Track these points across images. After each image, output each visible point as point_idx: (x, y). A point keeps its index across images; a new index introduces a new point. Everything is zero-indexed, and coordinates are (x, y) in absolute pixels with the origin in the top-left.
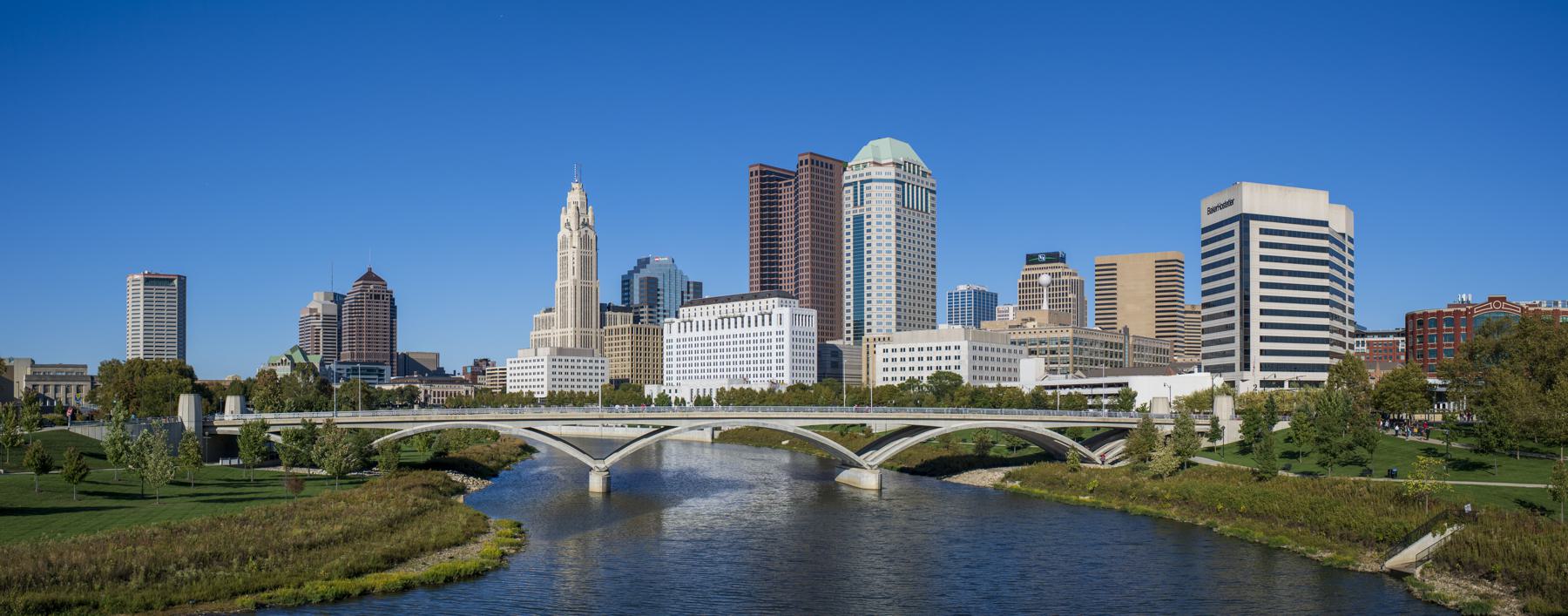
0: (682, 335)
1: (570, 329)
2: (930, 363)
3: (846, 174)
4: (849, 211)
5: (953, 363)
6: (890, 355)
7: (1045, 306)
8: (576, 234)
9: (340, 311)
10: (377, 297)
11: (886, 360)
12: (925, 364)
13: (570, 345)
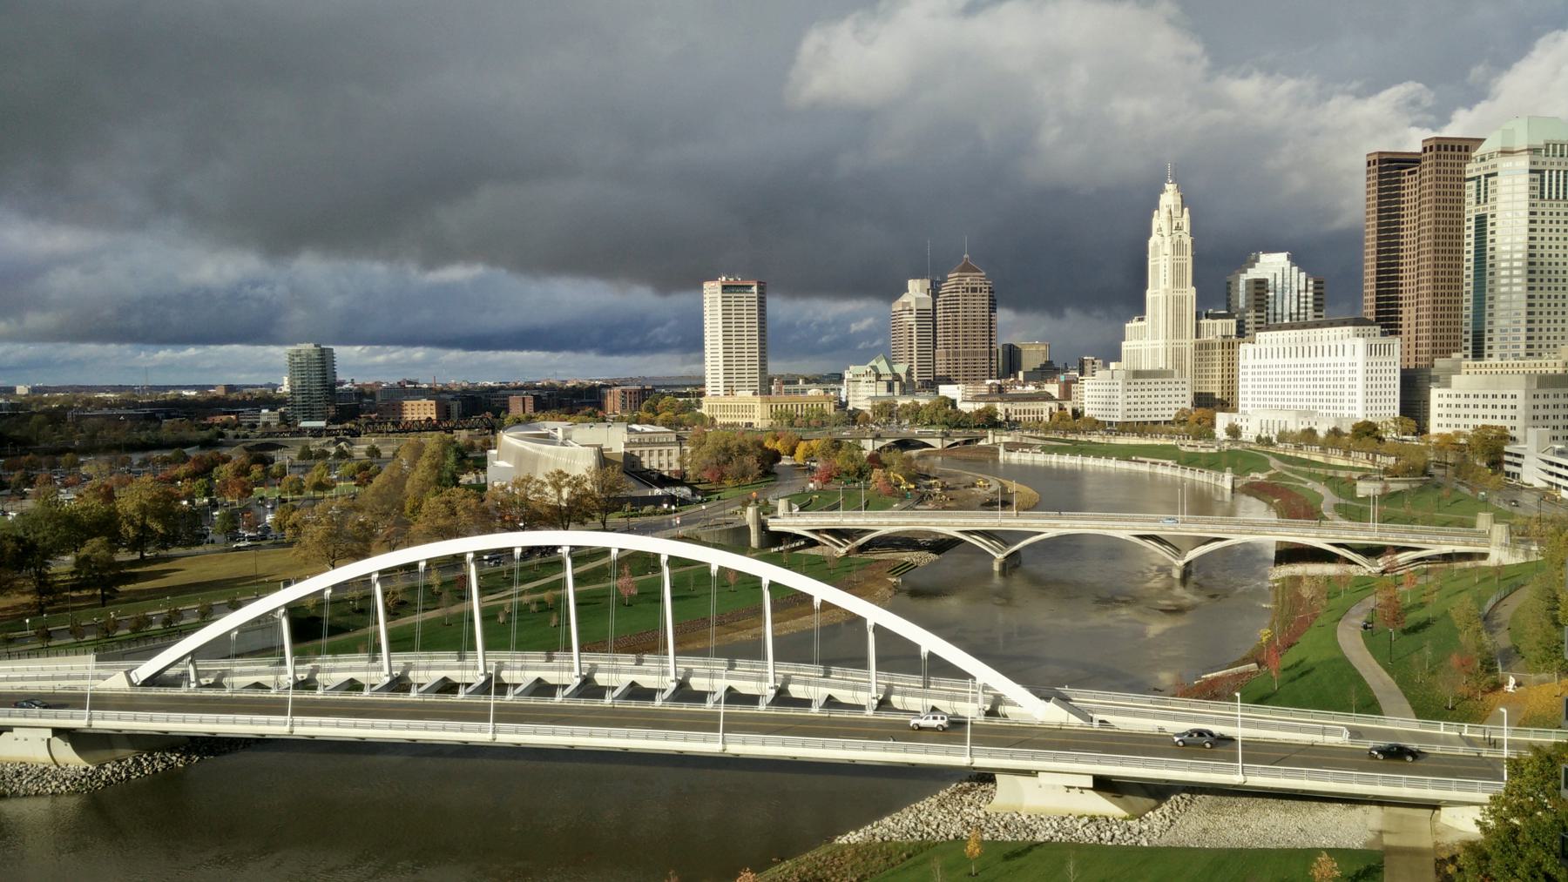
0: (1257, 362)
1: (1161, 342)
3: (1468, 167)
4: (1471, 210)
8: (1168, 240)
9: (934, 305)
10: (974, 290)
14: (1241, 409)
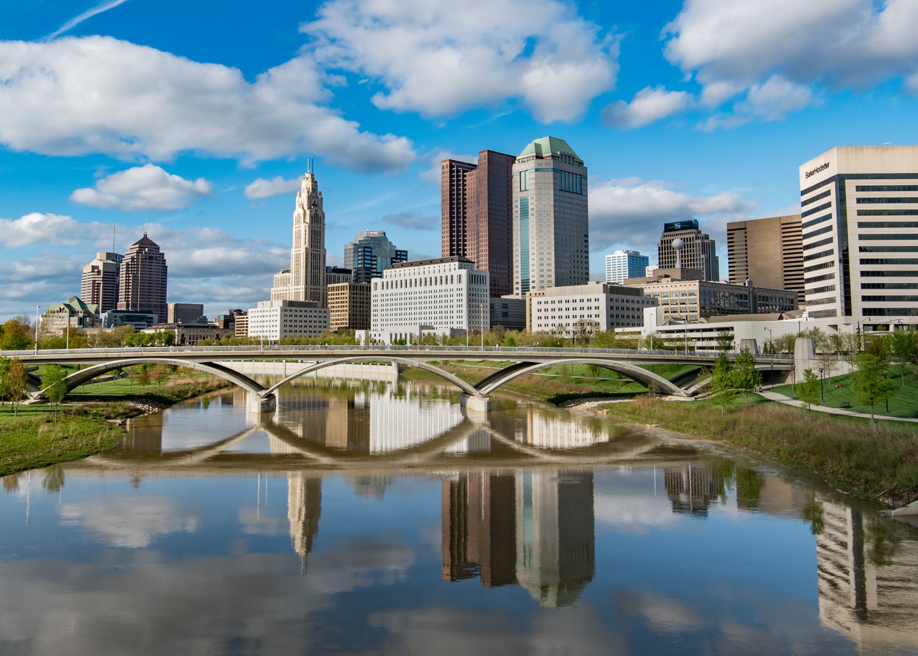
1: (302, 287)
2: (575, 313)
5: (593, 312)
6: (543, 306)
7: (678, 265)
11: (540, 310)
12: (571, 313)
13: (302, 298)
14: (372, 328)
